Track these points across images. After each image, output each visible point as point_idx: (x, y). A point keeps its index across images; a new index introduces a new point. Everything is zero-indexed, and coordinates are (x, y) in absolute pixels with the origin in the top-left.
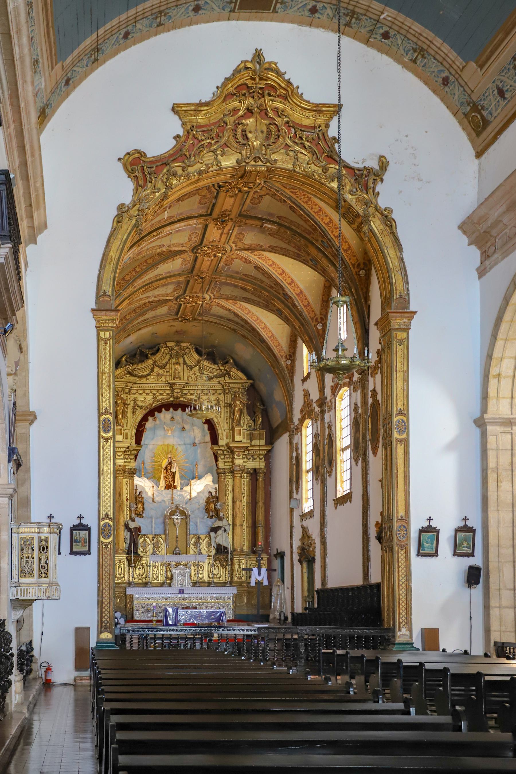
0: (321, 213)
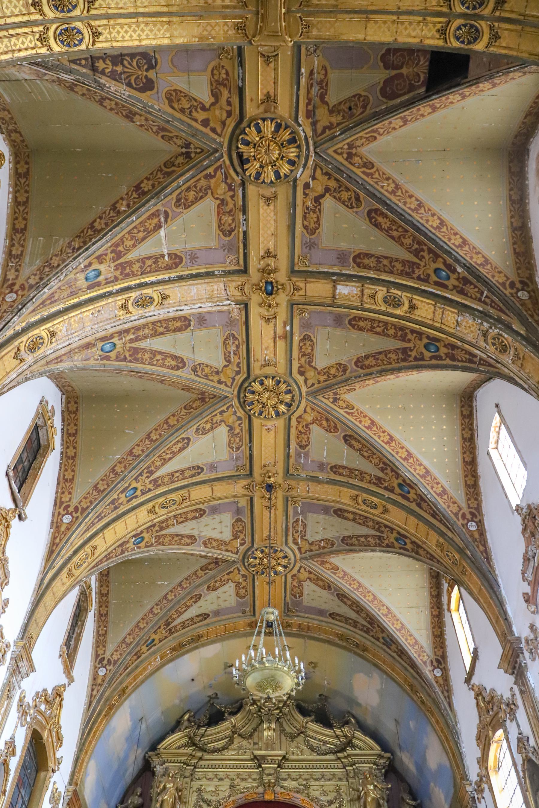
0: (422, 211)
